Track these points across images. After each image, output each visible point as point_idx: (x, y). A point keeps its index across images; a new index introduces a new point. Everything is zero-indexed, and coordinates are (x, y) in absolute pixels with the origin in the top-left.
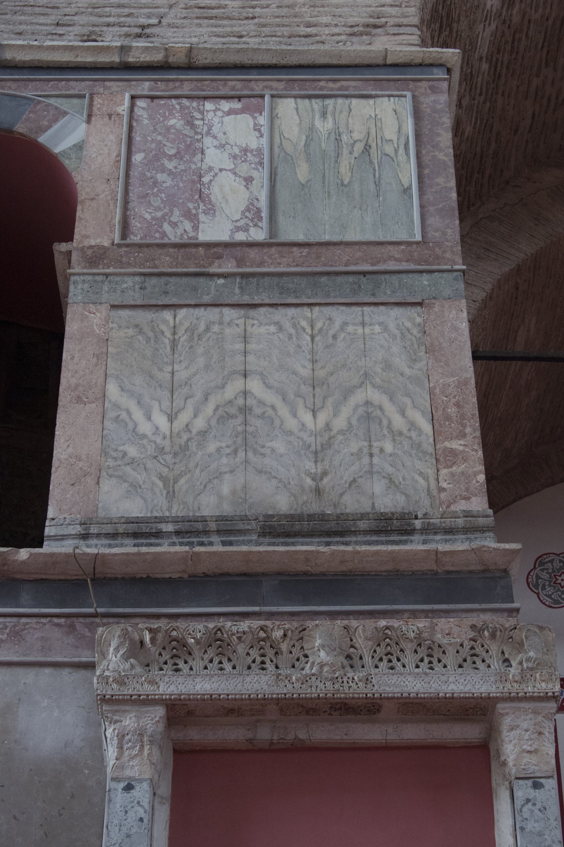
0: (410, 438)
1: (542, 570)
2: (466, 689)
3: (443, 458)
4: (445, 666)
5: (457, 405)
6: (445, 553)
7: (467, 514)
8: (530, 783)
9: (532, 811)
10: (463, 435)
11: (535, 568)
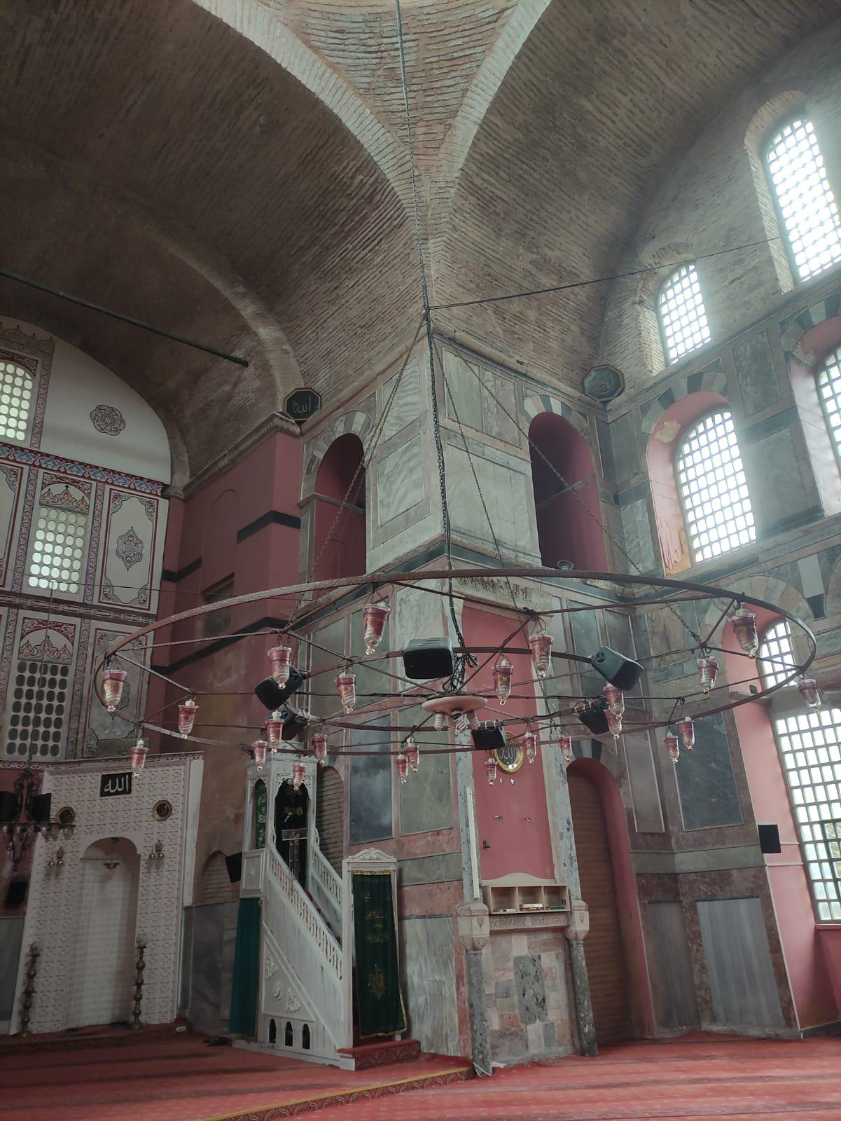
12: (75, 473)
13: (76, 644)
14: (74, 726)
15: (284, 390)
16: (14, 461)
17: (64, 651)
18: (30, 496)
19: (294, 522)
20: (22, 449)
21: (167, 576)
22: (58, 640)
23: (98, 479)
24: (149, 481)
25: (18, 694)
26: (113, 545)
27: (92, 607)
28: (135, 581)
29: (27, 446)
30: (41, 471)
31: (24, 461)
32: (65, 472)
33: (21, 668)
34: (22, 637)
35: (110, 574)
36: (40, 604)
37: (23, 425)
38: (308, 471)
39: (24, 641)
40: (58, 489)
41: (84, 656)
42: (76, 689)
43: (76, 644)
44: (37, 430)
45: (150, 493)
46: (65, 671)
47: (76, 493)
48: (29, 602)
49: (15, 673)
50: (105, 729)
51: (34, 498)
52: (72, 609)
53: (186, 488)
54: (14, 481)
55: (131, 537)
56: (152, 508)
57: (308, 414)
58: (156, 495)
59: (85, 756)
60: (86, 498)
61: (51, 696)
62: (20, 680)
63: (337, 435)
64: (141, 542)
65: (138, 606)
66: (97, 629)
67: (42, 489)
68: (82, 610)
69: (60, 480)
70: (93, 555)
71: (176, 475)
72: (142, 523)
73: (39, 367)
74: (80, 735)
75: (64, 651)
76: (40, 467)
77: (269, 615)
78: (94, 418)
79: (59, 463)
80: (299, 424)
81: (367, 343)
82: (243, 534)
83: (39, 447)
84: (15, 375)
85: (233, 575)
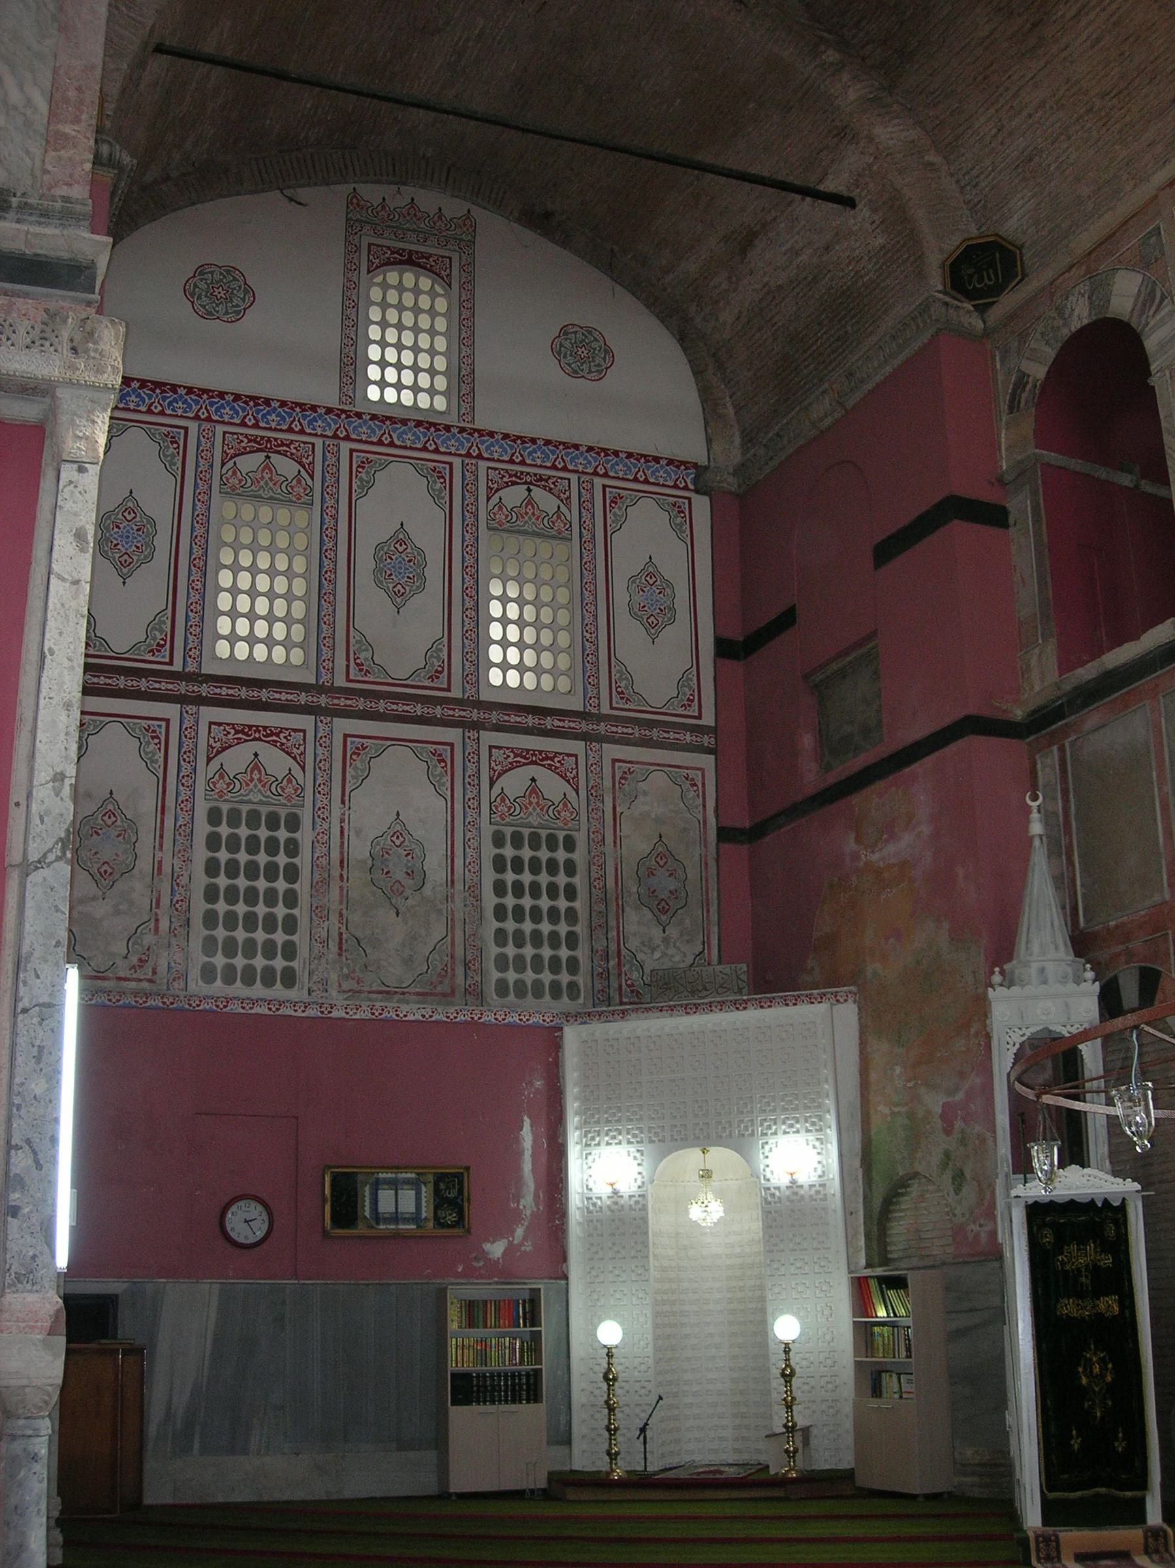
0: (25, 115)
1: (201, 280)
2: (29, 370)
3: (54, 141)
4: (13, 345)
5: (79, 89)
6: (36, 235)
7: (67, 199)
8: (75, 466)
9: (72, 492)
10: (77, 120)
11: (194, 276)
12: (539, 462)
13: (583, 792)
14: (600, 945)
15: (938, 249)
16: (437, 451)
17: (565, 805)
18: (470, 510)
19: (996, 516)
20: (448, 428)
21: (724, 649)
22: (552, 786)
23: (580, 468)
24: (670, 462)
25: (499, 888)
26: (621, 596)
27: (600, 718)
28: (667, 663)
29: (453, 420)
30: (483, 465)
31: (453, 450)
32: (523, 463)
33: (498, 841)
34: (492, 783)
35: (621, 652)
36: (513, 719)
37: (441, 383)
38: (1013, 406)
39: (496, 790)
40: (514, 496)
41: (600, 814)
42: (594, 875)
43: (583, 792)
44: (465, 389)
45: (675, 487)
46: (570, 844)
47: (546, 501)
48: (494, 717)
49: (489, 851)
50: (653, 950)
51: (476, 517)
52: (566, 724)
53: (740, 470)
54: (440, 491)
55: (650, 575)
56: (681, 514)
57: (997, 290)
58: (686, 488)
59: (625, 1000)
60: (563, 509)
61: (553, 891)
62: (499, 864)
63: (1075, 325)
64: (670, 585)
65: (680, 711)
66: (614, 761)
67: (488, 499)
68: (584, 726)
69: (515, 479)
70: (589, 619)
71: (716, 447)
72: (668, 547)
73: (455, 266)
74: (613, 963)
75: (565, 805)
76: (480, 457)
77: (972, 711)
78: (557, 351)
79: (511, 447)
80: (982, 309)
81: (1118, 126)
82: (885, 552)
83: (473, 421)
84: (417, 291)
85: (874, 634)
